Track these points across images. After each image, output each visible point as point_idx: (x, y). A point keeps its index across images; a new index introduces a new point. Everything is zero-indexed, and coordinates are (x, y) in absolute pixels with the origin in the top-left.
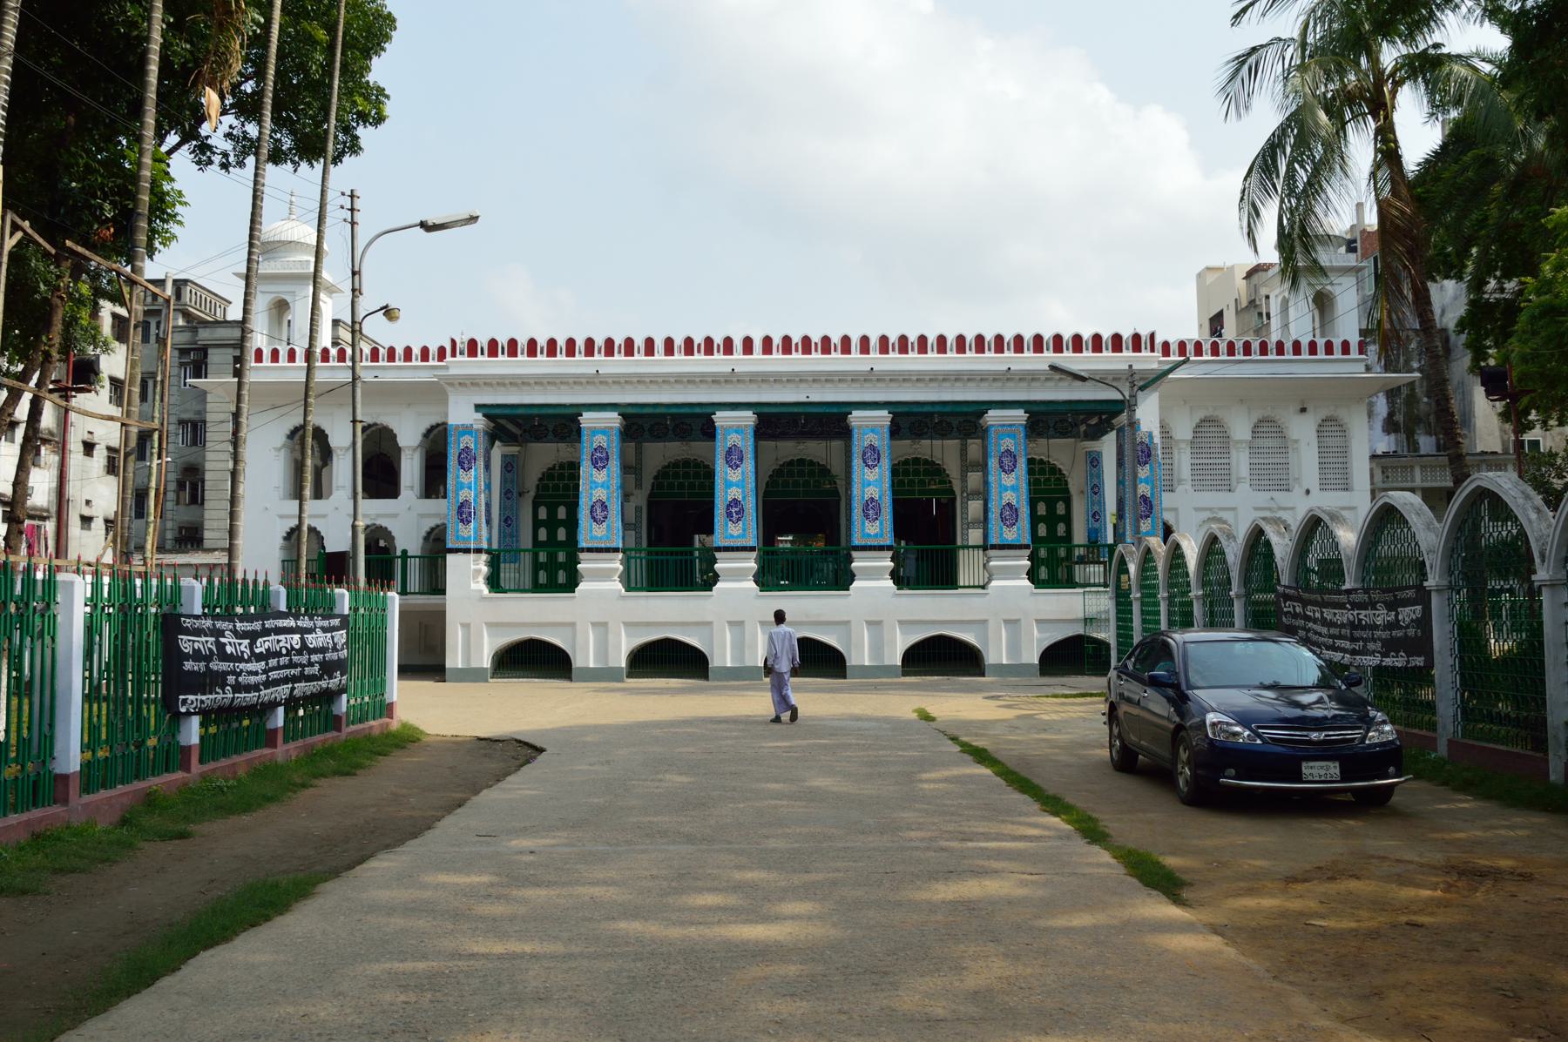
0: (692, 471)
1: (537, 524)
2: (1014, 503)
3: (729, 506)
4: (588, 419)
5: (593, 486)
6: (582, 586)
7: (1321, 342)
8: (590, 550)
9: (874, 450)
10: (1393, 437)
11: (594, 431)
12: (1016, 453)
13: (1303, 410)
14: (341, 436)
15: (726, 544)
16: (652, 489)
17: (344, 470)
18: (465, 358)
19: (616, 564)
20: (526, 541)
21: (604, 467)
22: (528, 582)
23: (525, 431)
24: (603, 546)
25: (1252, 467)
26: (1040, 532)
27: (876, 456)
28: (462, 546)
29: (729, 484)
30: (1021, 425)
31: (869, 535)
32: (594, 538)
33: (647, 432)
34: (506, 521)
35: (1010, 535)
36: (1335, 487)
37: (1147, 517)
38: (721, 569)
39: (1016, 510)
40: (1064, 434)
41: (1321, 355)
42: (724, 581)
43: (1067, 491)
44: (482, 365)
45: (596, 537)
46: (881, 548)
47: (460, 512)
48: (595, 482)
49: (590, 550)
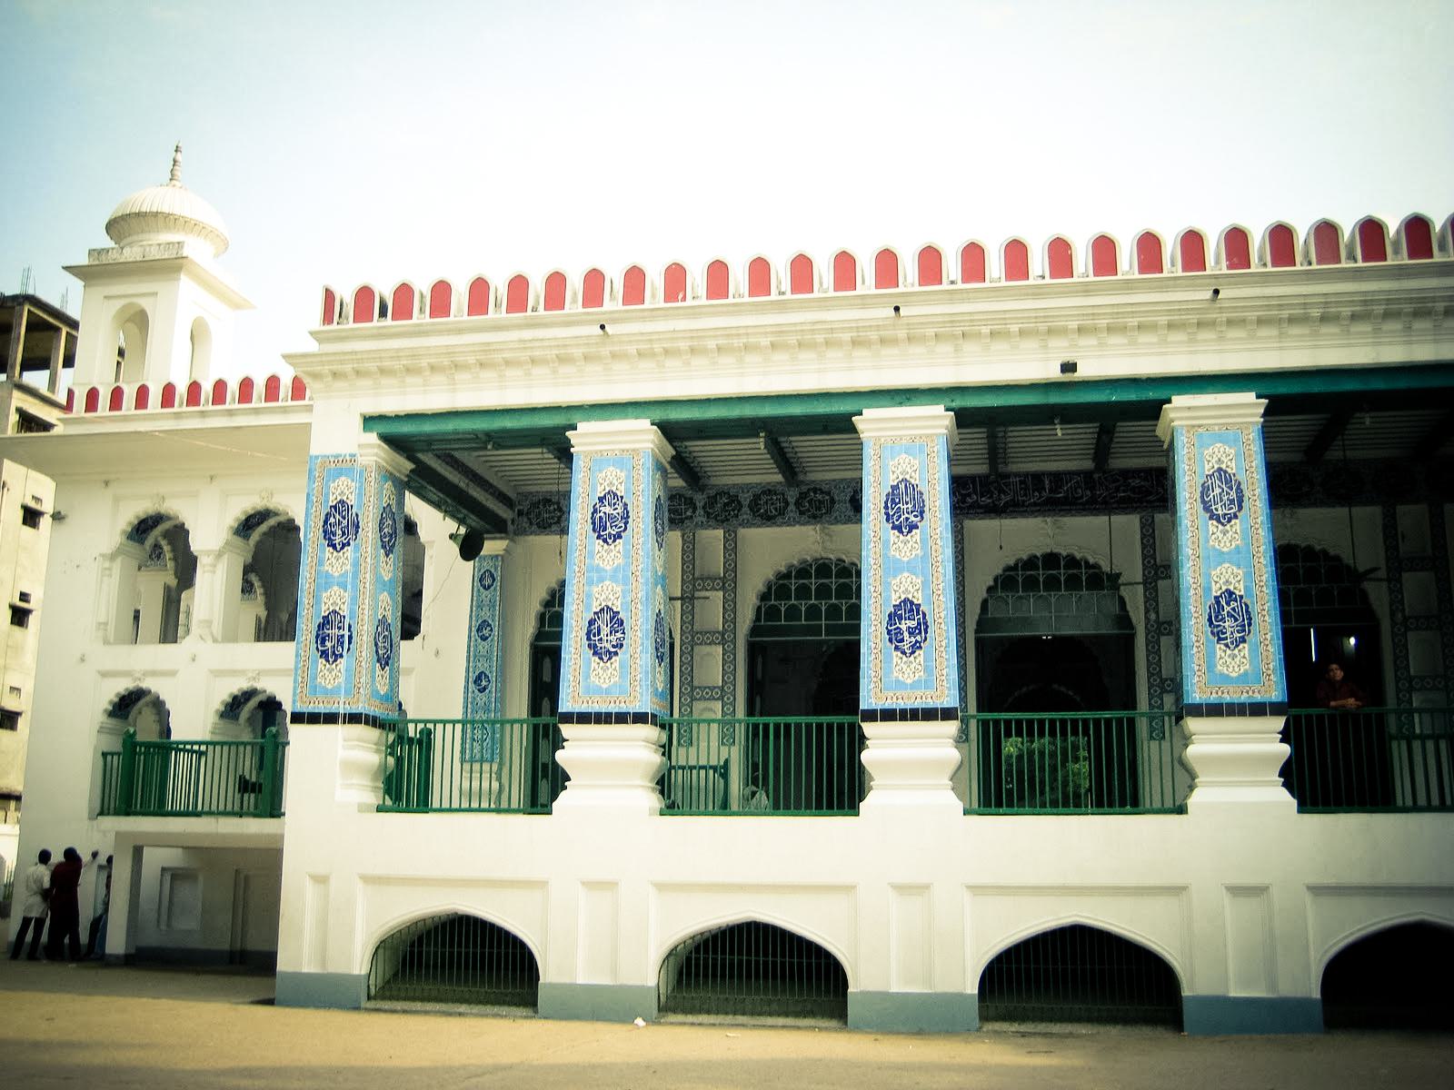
0: (833, 583)
5: (595, 576)
8: (584, 718)
9: (1228, 481)
11: (599, 460)
16: (758, 618)
23: (520, 513)
24: (613, 709)
27: (1233, 495)
29: (893, 568)
31: (1226, 678)
33: (745, 509)
34: (478, 680)
45: (599, 690)
46: (1257, 710)
48: (598, 569)
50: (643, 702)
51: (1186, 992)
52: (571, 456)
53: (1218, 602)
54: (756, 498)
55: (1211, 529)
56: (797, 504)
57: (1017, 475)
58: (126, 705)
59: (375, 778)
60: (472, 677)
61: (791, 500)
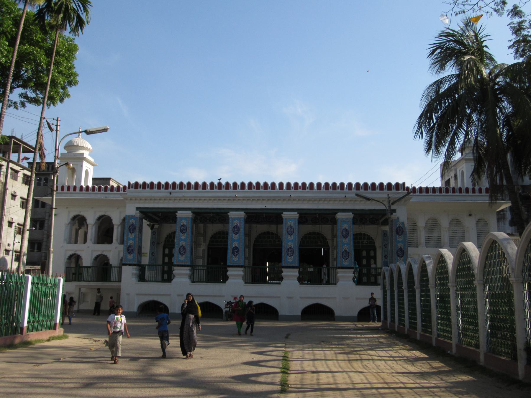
1: (164, 255)
2: (348, 250)
4: (179, 214)
6: (175, 280)
7: (477, 188)
10: (513, 227)
11: (182, 218)
13: (470, 215)
14: (91, 219)
15: (232, 264)
17: (92, 232)
18: (141, 189)
20: (160, 262)
21: (185, 233)
22: (160, 278)
25: (450, 238)
26: (363, 262)
28: (128, 263)
30: (351, 219)
35: (346, 263)
37: (402, 256)
39: (348, 253)
40: (373, 224)
41: (477, 193)
43: (375, 246)
44: (140, 192)
47: (128, 250)
49: (178, 266)
50: (189, 263)
51: (279, 314)
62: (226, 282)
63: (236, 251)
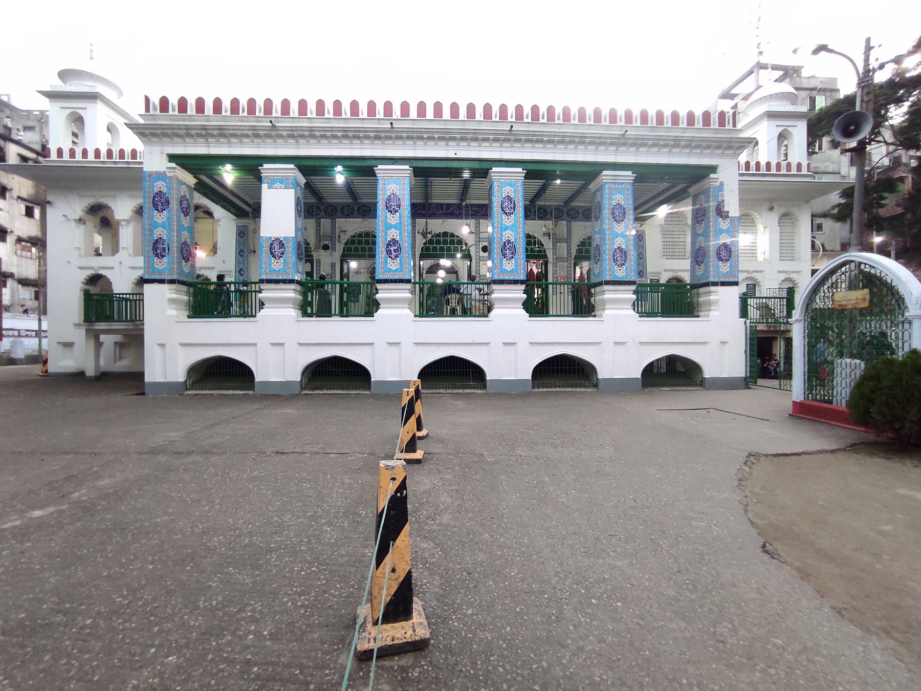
3: (388, 245)
12: (625, 206)
19: (291, 293)
24: (280, 278)
27: (512, 205)
28: (157, 277)
29: (388, 227)
32: (273, 271)
35: (620, 273)
36: (787, 258)
37: (727, 260)
38: (382, 299)
39: (625, 252)
42: (383, 308)
46: (516, 282)
47: (155, 249)
51: (488, 378)
52: (261, 177)
53: (505, 244)
54: (343, 207)
55: (504, 217)
56: (358, 210)
57: (434, 204)
58: (95, 279)
59: (186, 306)
60: (237, 270)
61: (356, 209)
62: (375, 314)
63: (393, 247)
